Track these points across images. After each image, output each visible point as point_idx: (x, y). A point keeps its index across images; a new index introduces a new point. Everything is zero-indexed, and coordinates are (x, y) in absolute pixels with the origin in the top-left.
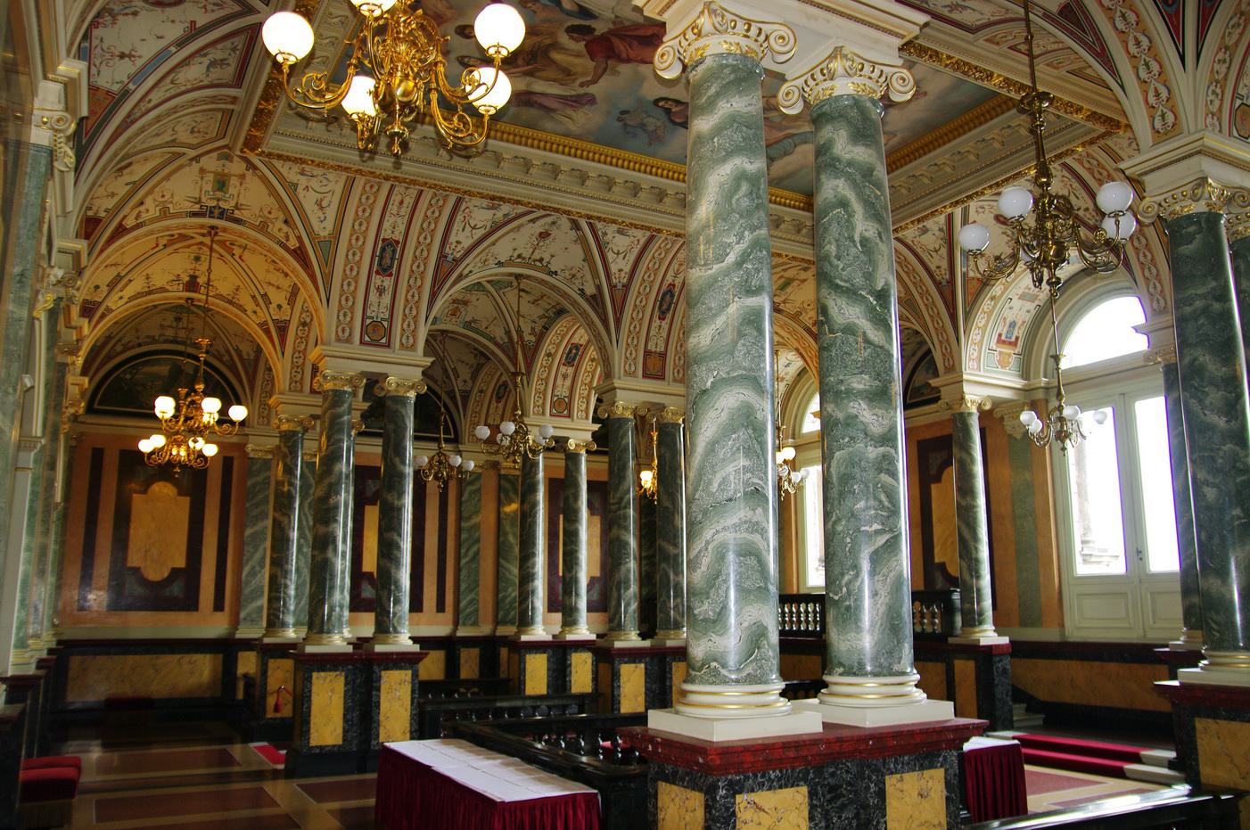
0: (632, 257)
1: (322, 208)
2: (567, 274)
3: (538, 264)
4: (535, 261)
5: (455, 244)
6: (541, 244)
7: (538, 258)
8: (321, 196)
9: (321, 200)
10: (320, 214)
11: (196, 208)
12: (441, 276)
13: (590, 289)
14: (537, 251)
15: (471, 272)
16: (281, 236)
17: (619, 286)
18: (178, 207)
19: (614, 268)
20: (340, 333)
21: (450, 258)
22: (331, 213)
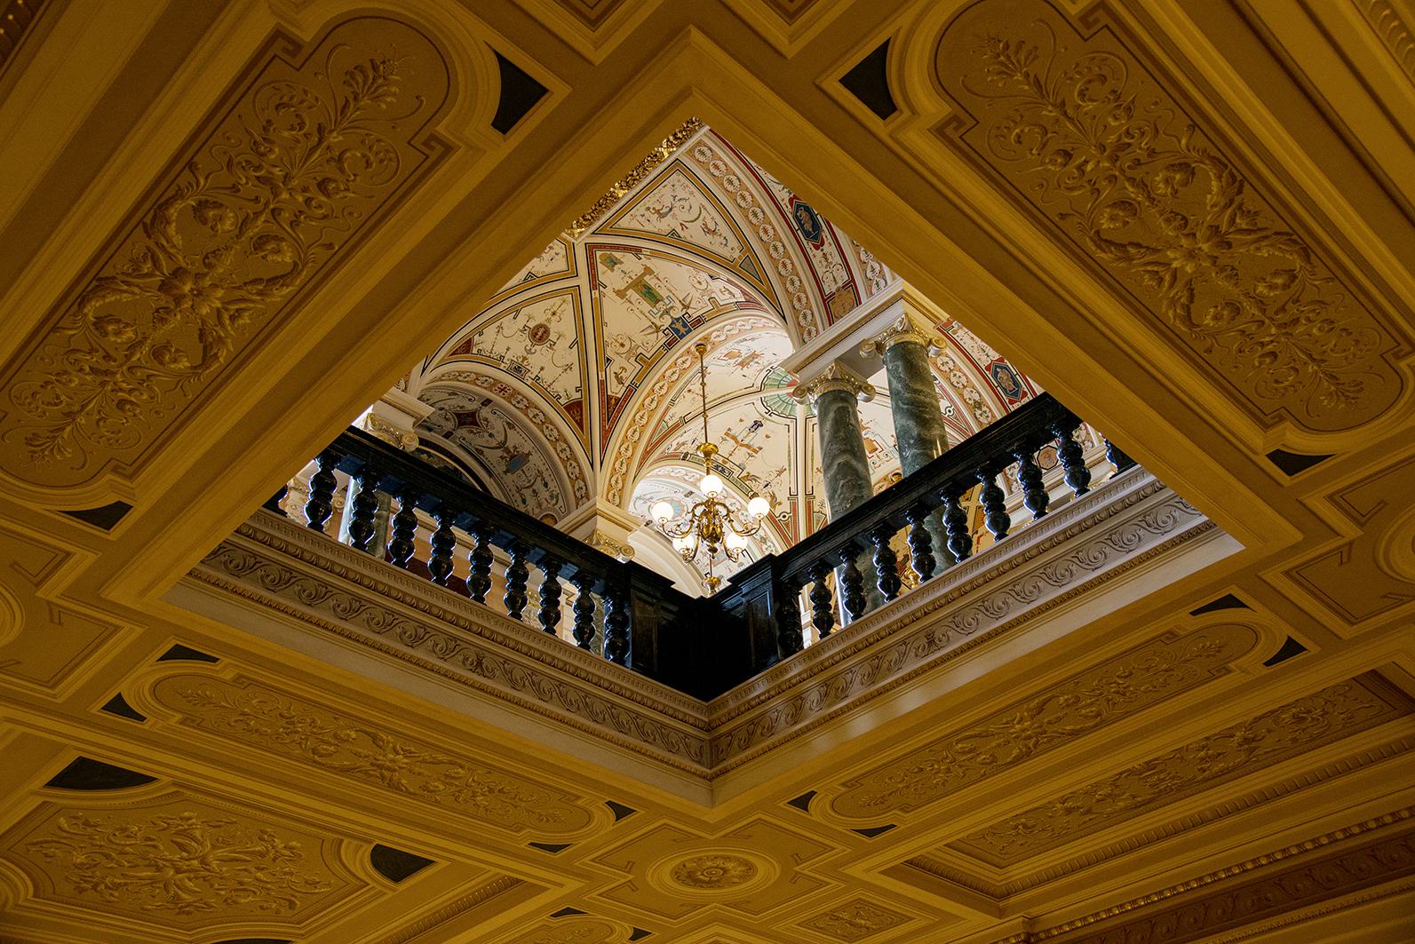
8: (700, 222)
9: (705, 225)
22: (723, 229)
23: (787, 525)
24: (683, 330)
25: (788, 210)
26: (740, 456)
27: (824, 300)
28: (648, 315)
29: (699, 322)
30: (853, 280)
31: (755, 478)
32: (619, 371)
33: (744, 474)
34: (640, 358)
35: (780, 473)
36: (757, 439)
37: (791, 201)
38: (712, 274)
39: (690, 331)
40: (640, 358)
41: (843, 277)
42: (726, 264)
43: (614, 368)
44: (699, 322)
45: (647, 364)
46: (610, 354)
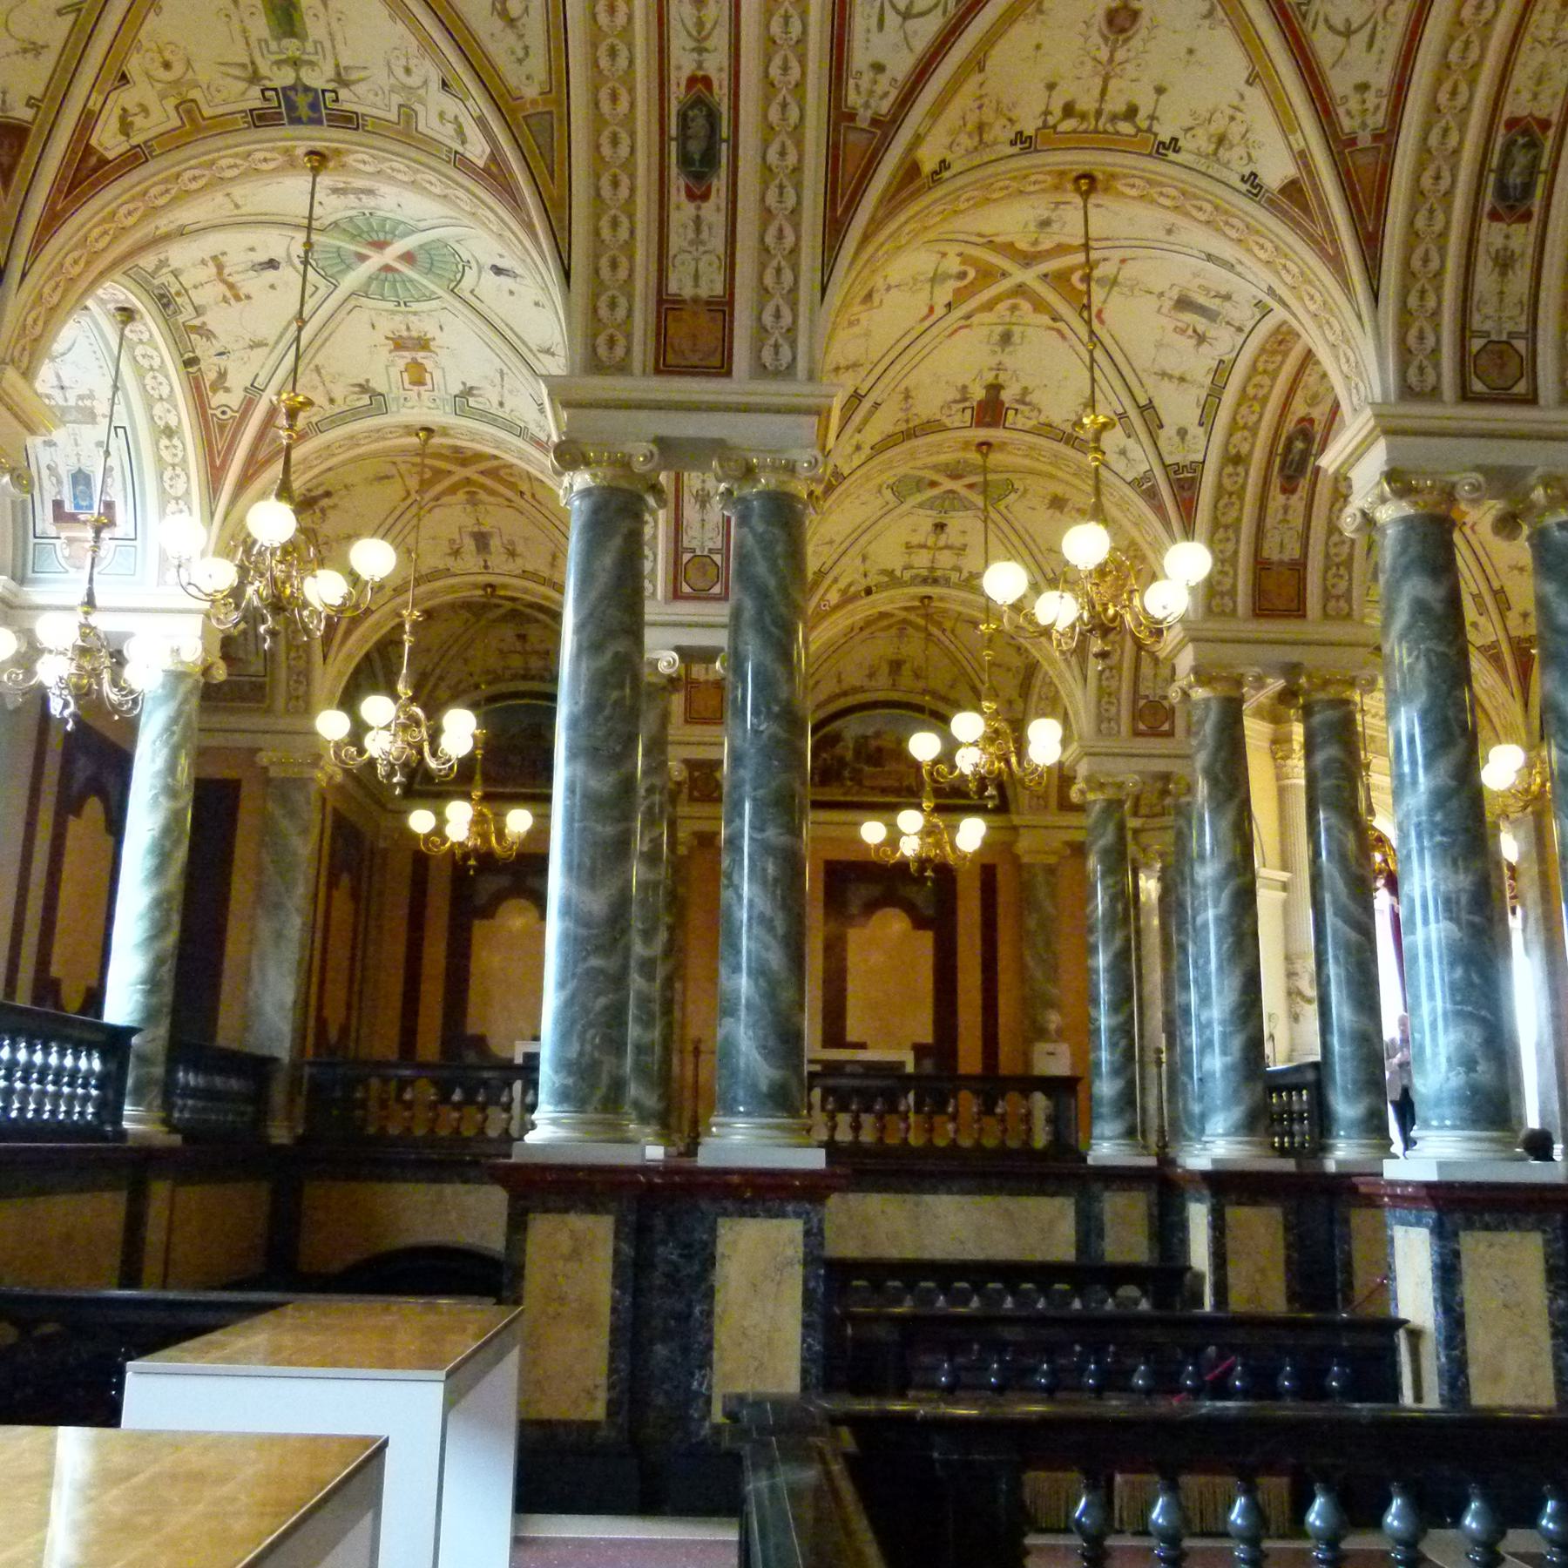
0: (1391, 39)
1: (512, 23)
2: (1203, 142)
3: (1125, 128)
4: (1114, 118)
5: (868, 76)
6: (1120, 55)
7: (1121, 107)
10: (511, 38)
11: (253, 99)
12: (850, 169)
13: (1277, 170)
14: (1114, 84)
15: (944, 165)
16: (445, 135)
17: (1365, 139)
18: (219, 98)
19: (1339, 83)
20: (602, 351)
21: (863, 122)
22: (535, 28)
23: (222, 427)
24: (304, 112)
25: (677, 93)
26: (209, 294)
27: (660, 302)
28: (254, 44)
29: (348, 120)
30: (731, 302)
31: (208, 334)
32: (132, 109)
33: (197, 322)
34: (187, 109)
35: (255, 345)
36: (253, 284)
37: (692, 81)
38: (450, 81)
39: (319, 122)
40: (187, 109)
41: (712, 285)
42: (501, 100)
43: (127, 98)
44: (348, 120)
45: (194, 125)
46: (134, 66)
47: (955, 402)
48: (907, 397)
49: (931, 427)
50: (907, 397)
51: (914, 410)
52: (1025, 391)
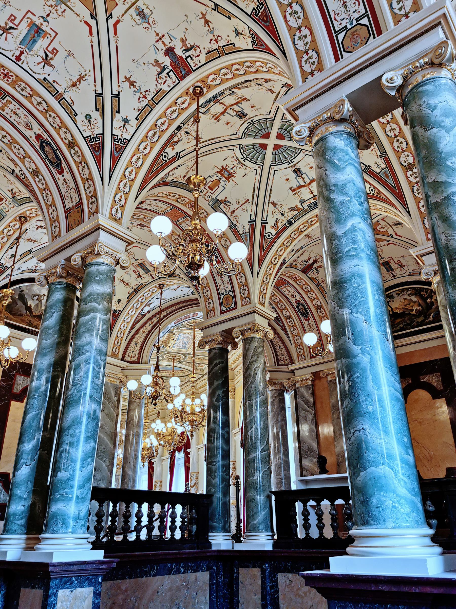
47: (160, 73)
48: (132, 84)
49: (160, 95)
50: (132, 84)
51: (143, 90)
52: (183, 41)
